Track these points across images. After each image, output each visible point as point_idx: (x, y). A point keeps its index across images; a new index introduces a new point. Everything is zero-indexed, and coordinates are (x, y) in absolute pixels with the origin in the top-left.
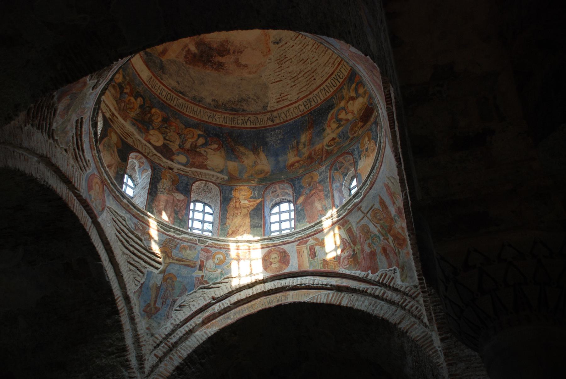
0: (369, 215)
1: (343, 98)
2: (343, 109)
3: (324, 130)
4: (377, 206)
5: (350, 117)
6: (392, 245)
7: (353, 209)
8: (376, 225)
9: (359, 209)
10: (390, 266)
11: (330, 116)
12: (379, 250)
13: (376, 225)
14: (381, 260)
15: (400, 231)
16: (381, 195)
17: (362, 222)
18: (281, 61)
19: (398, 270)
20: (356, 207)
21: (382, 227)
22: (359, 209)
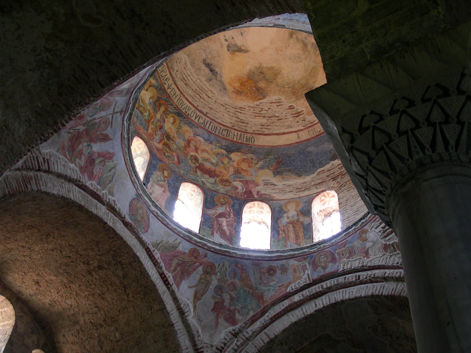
0: (110, 117)
7: (126, 108)
8: (99, 120)
13: (99, 120)
20: (125, 110)
22: (121, 112)
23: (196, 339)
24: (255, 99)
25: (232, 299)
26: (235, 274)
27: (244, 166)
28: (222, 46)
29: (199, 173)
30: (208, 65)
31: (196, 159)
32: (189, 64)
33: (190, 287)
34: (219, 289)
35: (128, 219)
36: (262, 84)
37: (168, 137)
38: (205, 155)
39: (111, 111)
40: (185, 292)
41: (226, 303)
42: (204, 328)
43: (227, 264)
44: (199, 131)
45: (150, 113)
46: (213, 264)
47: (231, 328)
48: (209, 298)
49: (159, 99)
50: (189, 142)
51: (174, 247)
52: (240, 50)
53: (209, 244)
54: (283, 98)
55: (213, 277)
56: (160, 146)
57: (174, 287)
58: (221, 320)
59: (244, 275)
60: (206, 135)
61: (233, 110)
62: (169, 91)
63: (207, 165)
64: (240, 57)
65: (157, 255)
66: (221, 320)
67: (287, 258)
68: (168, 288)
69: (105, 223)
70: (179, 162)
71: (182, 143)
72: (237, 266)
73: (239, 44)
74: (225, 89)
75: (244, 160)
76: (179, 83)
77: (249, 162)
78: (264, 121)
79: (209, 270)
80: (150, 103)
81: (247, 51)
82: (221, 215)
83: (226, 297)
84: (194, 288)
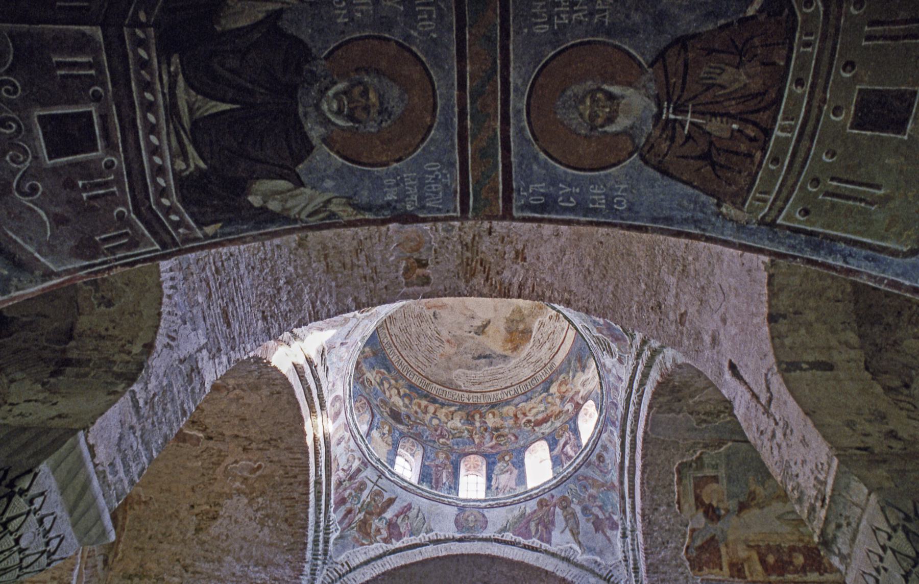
0: (376, 487)
1: (396, 381)
2: (390, 383)
3: (374, 368)
4: (386, 496)
5: (387, 394)
6: (357, 519)
9: (380, 477)
10: (340, 523)
11: (382, 370)
12: (348, 505)
14: (343, 510)
15: (374, 527)
16: (397, 500)
17: (368, 482)
18: (420, 316)
19: (338, 532)
21: (369, 503)
22: (380, 477)
23: (597, 570)
24: (528, 340)
25: (600, 508)
26: (585, 487)
27: (563, 389)
28: (472, 338)
29: (536, 429)
30: (479, 357)
31: (529, 421)
32: (467, 371)
33: (562, 532)
34: (585, 510)
35: (458, 536)
36: (521, 327)
37: (497, 429)
38: (534, 411)
39: (370, 485)
40: (561, 540)
41: (601, 516)
42: (601, 553)
43: (572, 486)
44: (516, 401)
45: (468, 431)
46: (564, 497)
47: (619, 533)
48: (585, 525)
49: (468, 414)
50: (516, 416)
51: (523, 515)
52: (485, 326)
53: (547, 486)
54: (540, 319)
55: (572, 506)
56: (494, 442)
57: (545, 546)
58: (609, 533)
59: (590, 481)
60: (524, 397)
61: (525, 362)
62: (471, 401)
63: (540, 417)
64: (490, 330)
65: (509, 536)
66: (609, 533)
67: (599, 438)
68: (540, 552)
69: (438, 557)
70: (517, 438)
71: (511, 422)
72: (579, 480)
73: (480, 324)
74: (506, 357)
75: (560, 385)
76: (473, 389)
77: (564, 382)
78: (547, 345)
79: (565, 503)
80: (463, 424)
81: (489, 322)
82: (564, 446)
83: (596, 511)
84: (567, 532)
